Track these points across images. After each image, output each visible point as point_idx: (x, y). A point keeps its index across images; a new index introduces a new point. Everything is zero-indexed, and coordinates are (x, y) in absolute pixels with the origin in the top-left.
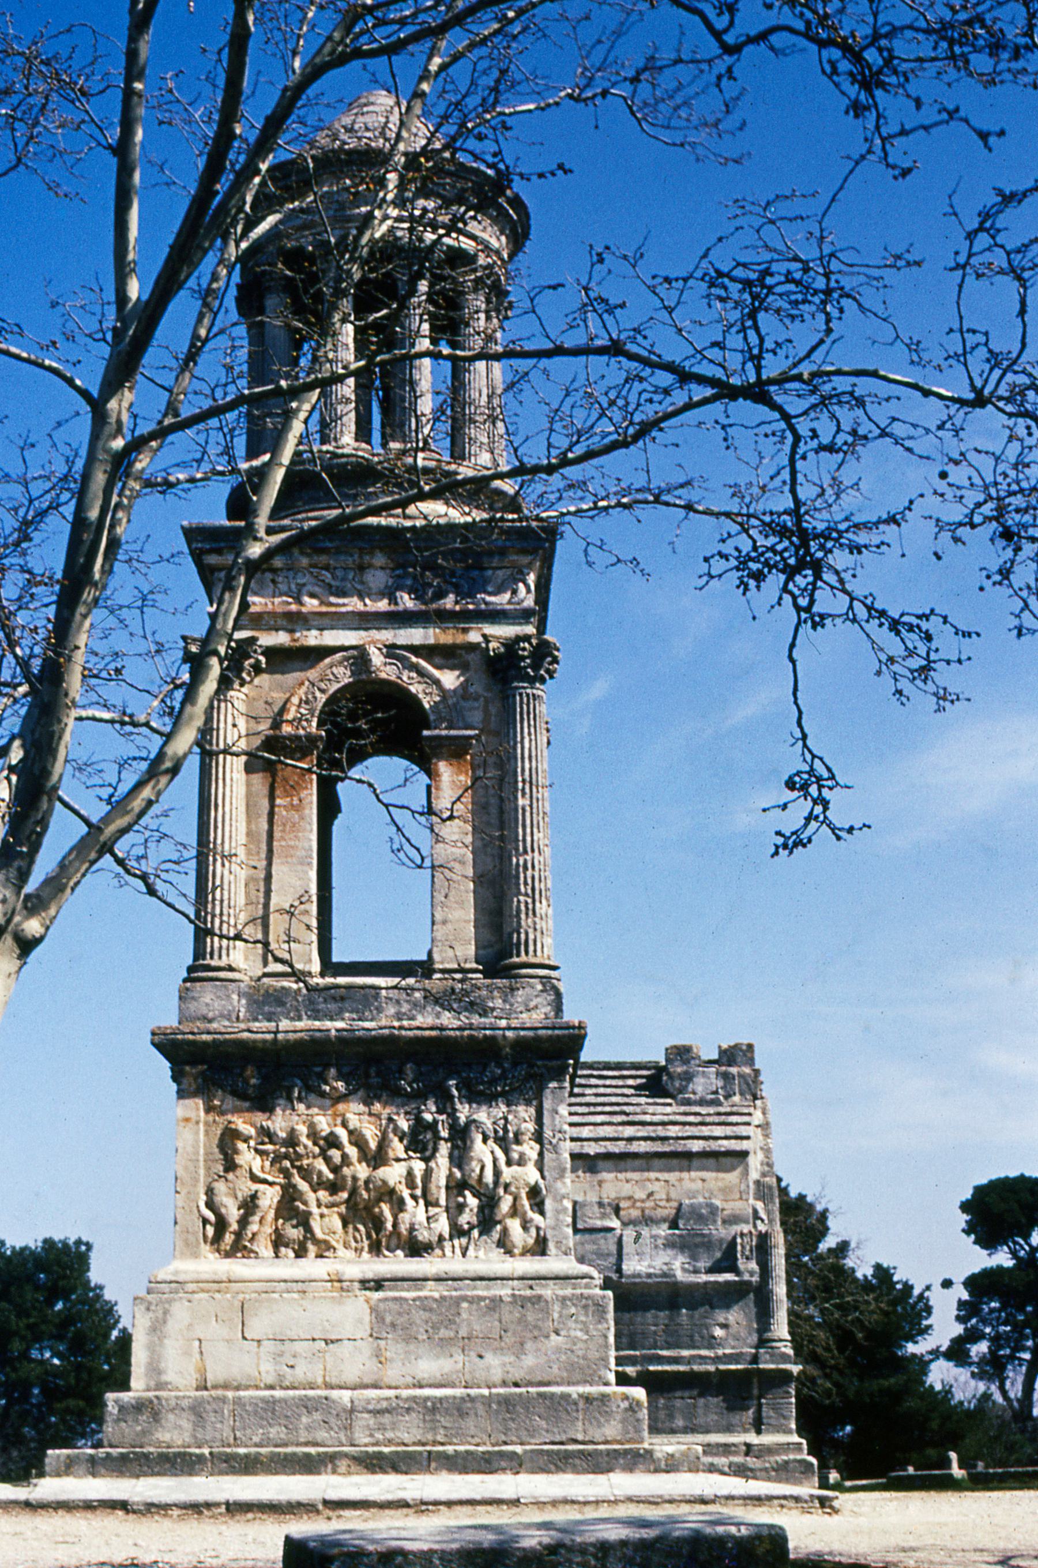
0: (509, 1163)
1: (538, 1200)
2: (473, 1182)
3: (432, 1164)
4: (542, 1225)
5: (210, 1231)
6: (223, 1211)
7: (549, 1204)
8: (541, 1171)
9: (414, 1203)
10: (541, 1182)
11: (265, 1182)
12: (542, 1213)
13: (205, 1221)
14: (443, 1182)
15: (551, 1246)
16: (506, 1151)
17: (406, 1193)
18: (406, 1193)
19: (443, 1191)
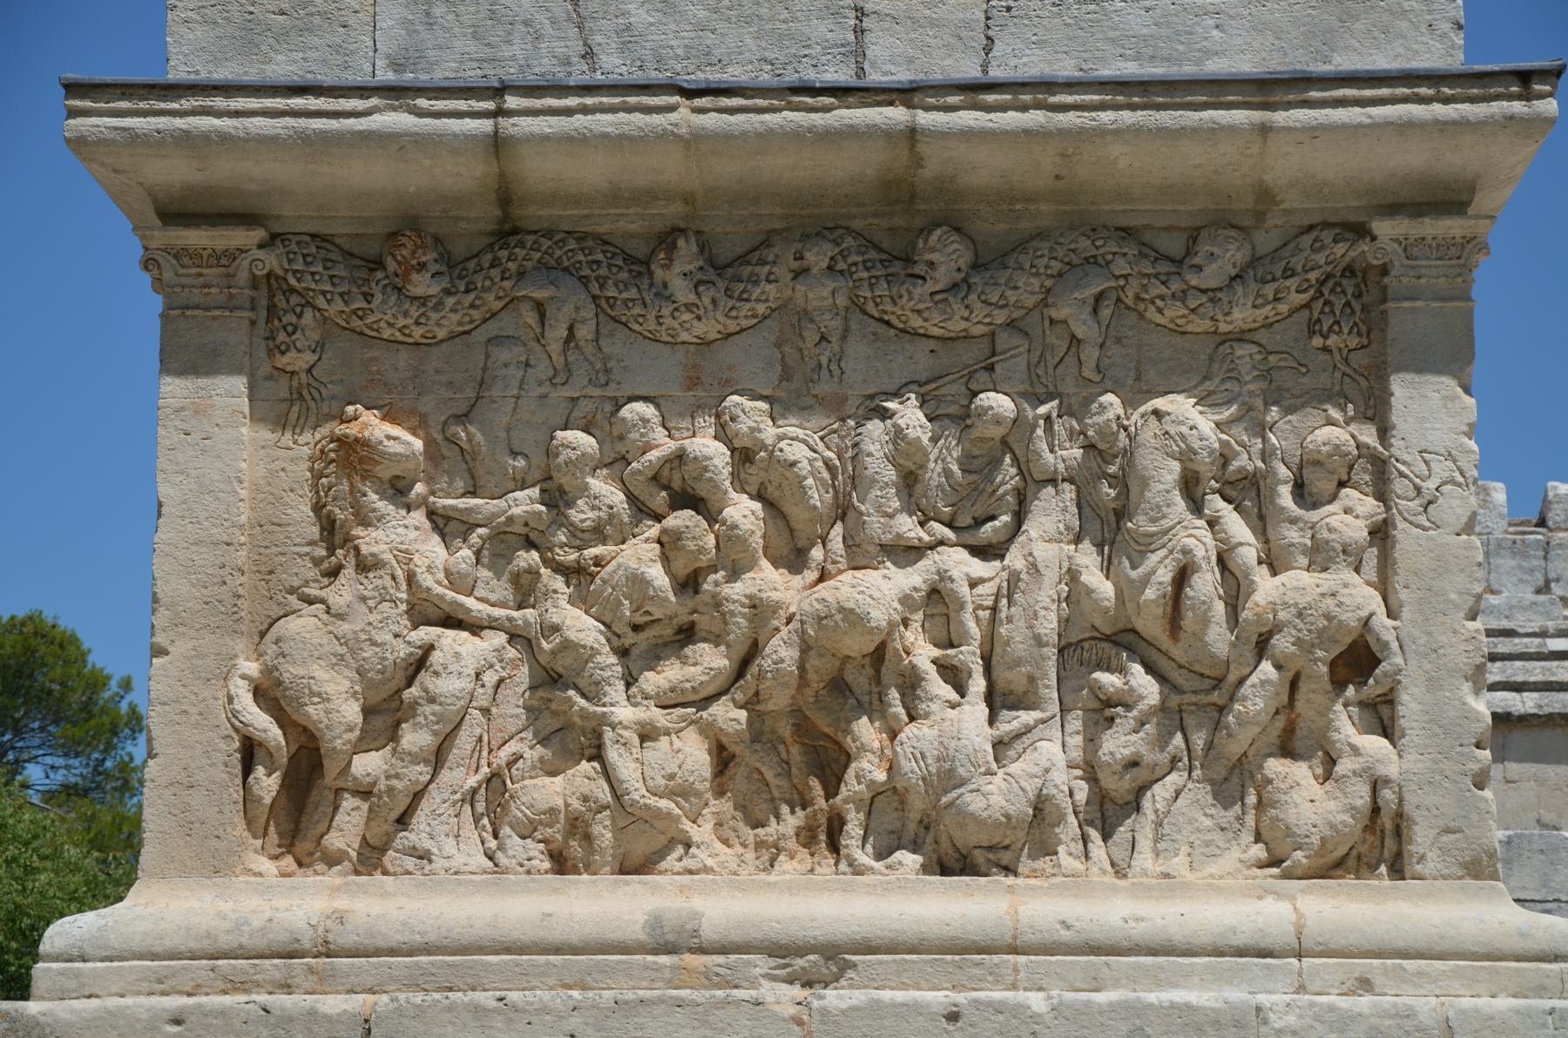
0: (1273, 562)
1: (1372, 688)
2: (1152, 625)
3: (1015, 558)
4: (1392, 769)
5: (267, 784)
6: (314, 711)
7: (1410, 706)
8: (1384, 586)
9: (948, 692)
10: (1382, 621)
11: (452, 621)
12: (1387, 729)
13: (250, 752)
14: (1049, 625)
15: (1422, 838)
16: (1261, 522)
17: (924, 654)
18: (924, 654)
19: (1052, 652)
